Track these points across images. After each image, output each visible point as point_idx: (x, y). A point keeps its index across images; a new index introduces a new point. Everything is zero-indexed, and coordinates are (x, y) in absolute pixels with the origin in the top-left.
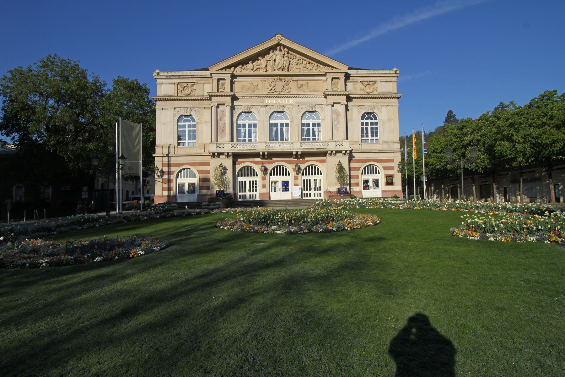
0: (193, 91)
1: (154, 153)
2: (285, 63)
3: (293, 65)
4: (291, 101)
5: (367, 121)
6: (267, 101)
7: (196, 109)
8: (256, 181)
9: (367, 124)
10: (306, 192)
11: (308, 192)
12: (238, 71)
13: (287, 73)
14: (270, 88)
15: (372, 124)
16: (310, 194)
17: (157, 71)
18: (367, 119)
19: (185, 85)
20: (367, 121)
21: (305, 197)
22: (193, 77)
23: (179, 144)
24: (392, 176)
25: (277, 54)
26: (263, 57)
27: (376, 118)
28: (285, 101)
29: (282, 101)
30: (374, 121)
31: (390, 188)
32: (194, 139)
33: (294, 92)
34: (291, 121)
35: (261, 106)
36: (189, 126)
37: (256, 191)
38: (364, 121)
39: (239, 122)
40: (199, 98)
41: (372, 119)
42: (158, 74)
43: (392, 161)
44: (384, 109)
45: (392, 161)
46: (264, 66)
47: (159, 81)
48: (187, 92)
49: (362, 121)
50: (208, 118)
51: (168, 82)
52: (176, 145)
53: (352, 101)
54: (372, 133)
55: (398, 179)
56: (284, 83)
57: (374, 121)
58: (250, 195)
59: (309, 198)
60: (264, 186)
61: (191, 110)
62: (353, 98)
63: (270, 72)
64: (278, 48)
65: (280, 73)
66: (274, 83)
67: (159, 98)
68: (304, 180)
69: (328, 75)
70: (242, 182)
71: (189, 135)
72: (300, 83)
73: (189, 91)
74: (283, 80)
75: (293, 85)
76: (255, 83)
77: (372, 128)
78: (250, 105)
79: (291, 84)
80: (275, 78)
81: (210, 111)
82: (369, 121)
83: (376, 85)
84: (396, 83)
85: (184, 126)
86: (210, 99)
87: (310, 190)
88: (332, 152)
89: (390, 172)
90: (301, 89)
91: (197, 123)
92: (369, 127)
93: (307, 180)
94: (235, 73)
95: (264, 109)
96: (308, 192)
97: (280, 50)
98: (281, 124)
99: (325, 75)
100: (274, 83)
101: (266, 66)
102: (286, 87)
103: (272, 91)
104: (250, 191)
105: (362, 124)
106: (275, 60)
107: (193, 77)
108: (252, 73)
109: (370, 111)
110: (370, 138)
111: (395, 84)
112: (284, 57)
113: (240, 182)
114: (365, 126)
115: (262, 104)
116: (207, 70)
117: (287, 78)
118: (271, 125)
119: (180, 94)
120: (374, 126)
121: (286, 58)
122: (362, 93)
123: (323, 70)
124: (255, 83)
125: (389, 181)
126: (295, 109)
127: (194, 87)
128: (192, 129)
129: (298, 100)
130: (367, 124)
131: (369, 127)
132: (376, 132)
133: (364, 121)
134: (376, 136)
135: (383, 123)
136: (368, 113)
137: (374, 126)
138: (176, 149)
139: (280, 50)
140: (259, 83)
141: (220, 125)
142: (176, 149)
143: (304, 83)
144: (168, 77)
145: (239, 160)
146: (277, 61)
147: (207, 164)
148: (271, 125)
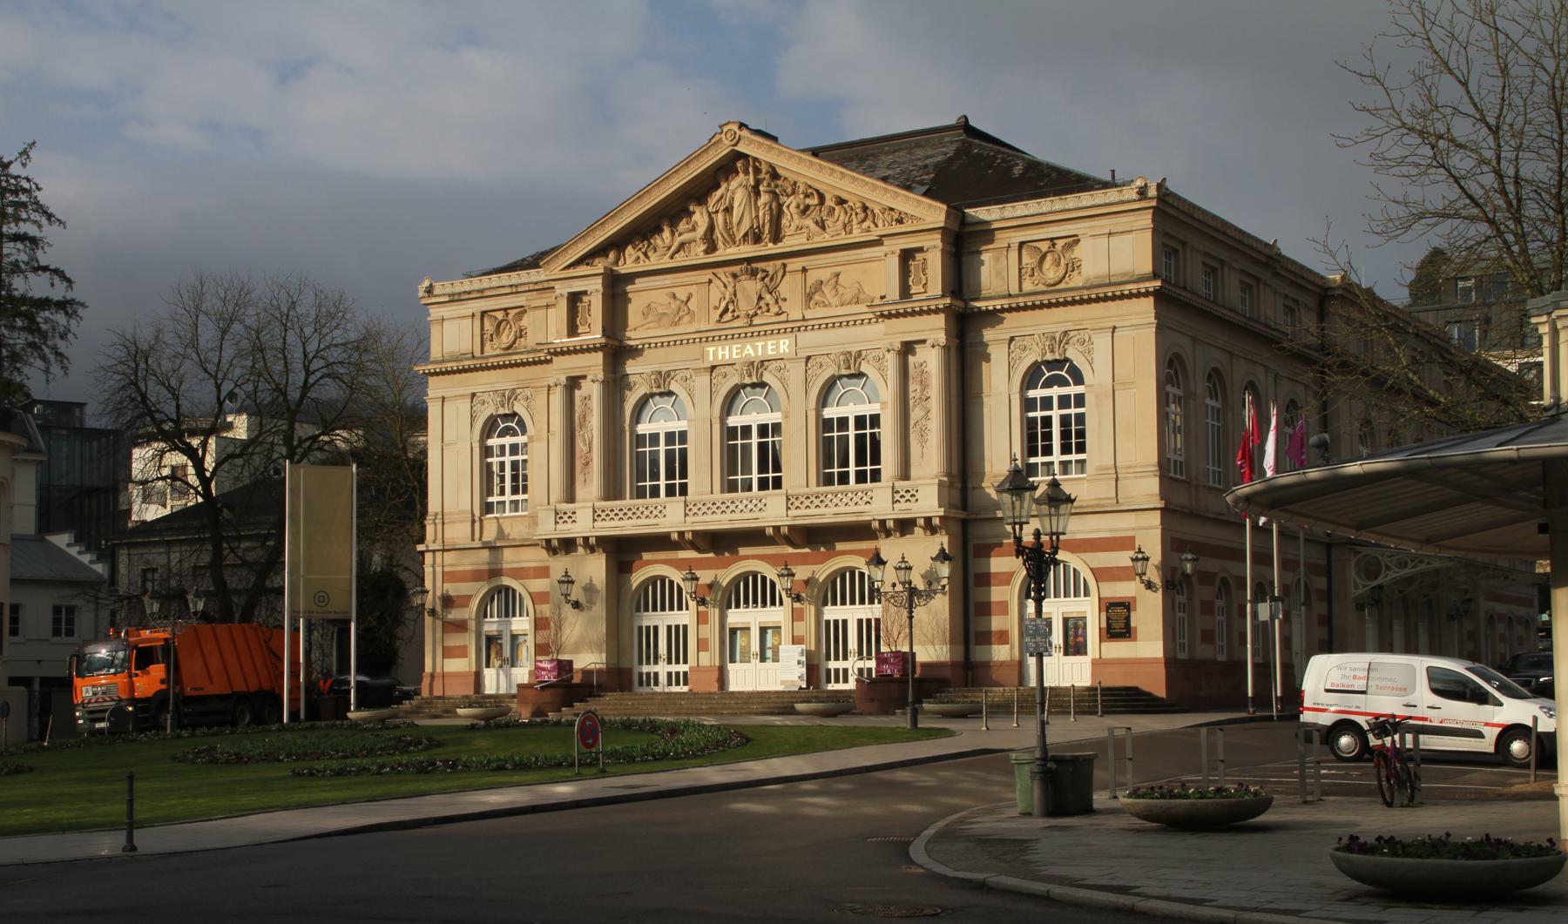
0: (521, 334)
1: (422, 540)
3: (791, 220)
4: (784, 345)
5: (1046, 392)
7: (528, 392)
8: (685, 627)
9: (1047, 403)
11: (841, 664)
12: (630, 261)
13: (770, 248)
15: (1064, 401)
17: (426, 283)
18: (1048, 384)
19: (500, 315)
20: (1046, 392)
21: (837, 681)
22: (515, 290)
24: (1126, 606)
25: (736, 189)
26: (702, 201)
27: (1079, 380)
28: (764, 348)
29: (755, 349)
30: (1072, 390)
32: (525, 491)
34: (786, 416)
37: (685, 662)
38: (1036, 393)
39: (643, 429)
41: (1062, 382)
42: (429, 291)
46: (701, 231)
47: (435, 313)
48: (506, 338)
49: (1032, 394)
52: (477, 513)
53: (1001, 321)
54: (1065, 435)
55: (1149, 612)
56: (759, 285)
57: (1072, 390)
58: (669, 674)
60: (702, 645)
61: (513, 395)
62: (1003, 310)
63: (725, 253)
64: (739, 164)
65: (748, 250)
66: (730, 289)
67: (438, 368)
68: (828, 622)
69: (886, 242)
70: (677, 627)
72: (813, 276)
73: (512, 337)
76: (682, 294)
77: (1065, 421)
78: (664, 370)
80: (736, 269)
82: (1055, 392)
83: (1078, 252)
84: (1148, 235)
87: (845, 658)
88: (882, 522)
90: (817, 297)
92: (1055, 414)
93: (836, 622)
94: (623, 269)
96: (841, 664)
98: (667, 434)
99: (878, 242)
101: (711, 228)
102: (768, 297)
103: (729, 316)
104: (670, 662)
105: (1029, 404)
106: (728, 210)
107: (515, 290)
108: (667, 263)
111: (1146, 240)
112: (758, 194)
115: (700, 365)
116: (533, 263)
117: (770, 266)
119: (488, 351)
120: (1073, 411)
121: (764, 198)
122: (1028, 286)
125: (1119, 625)
126: (796, 372)
127: (524, 323)
129: (808, 339)
131: (1055, 414)
132: (1081, 434)
133: (1036, 393)
134: (1081, 448)
135: (1097, 396)
136: (1052, 365)
137: (1073, 411)
138: (477, 525)
139: (746, 173)
140: (693, 289)
141: (579, 444)
142: (477, 525)
143: (825, 275)
144: (455, 299)
145: (646, 556)
146: (736, 213)
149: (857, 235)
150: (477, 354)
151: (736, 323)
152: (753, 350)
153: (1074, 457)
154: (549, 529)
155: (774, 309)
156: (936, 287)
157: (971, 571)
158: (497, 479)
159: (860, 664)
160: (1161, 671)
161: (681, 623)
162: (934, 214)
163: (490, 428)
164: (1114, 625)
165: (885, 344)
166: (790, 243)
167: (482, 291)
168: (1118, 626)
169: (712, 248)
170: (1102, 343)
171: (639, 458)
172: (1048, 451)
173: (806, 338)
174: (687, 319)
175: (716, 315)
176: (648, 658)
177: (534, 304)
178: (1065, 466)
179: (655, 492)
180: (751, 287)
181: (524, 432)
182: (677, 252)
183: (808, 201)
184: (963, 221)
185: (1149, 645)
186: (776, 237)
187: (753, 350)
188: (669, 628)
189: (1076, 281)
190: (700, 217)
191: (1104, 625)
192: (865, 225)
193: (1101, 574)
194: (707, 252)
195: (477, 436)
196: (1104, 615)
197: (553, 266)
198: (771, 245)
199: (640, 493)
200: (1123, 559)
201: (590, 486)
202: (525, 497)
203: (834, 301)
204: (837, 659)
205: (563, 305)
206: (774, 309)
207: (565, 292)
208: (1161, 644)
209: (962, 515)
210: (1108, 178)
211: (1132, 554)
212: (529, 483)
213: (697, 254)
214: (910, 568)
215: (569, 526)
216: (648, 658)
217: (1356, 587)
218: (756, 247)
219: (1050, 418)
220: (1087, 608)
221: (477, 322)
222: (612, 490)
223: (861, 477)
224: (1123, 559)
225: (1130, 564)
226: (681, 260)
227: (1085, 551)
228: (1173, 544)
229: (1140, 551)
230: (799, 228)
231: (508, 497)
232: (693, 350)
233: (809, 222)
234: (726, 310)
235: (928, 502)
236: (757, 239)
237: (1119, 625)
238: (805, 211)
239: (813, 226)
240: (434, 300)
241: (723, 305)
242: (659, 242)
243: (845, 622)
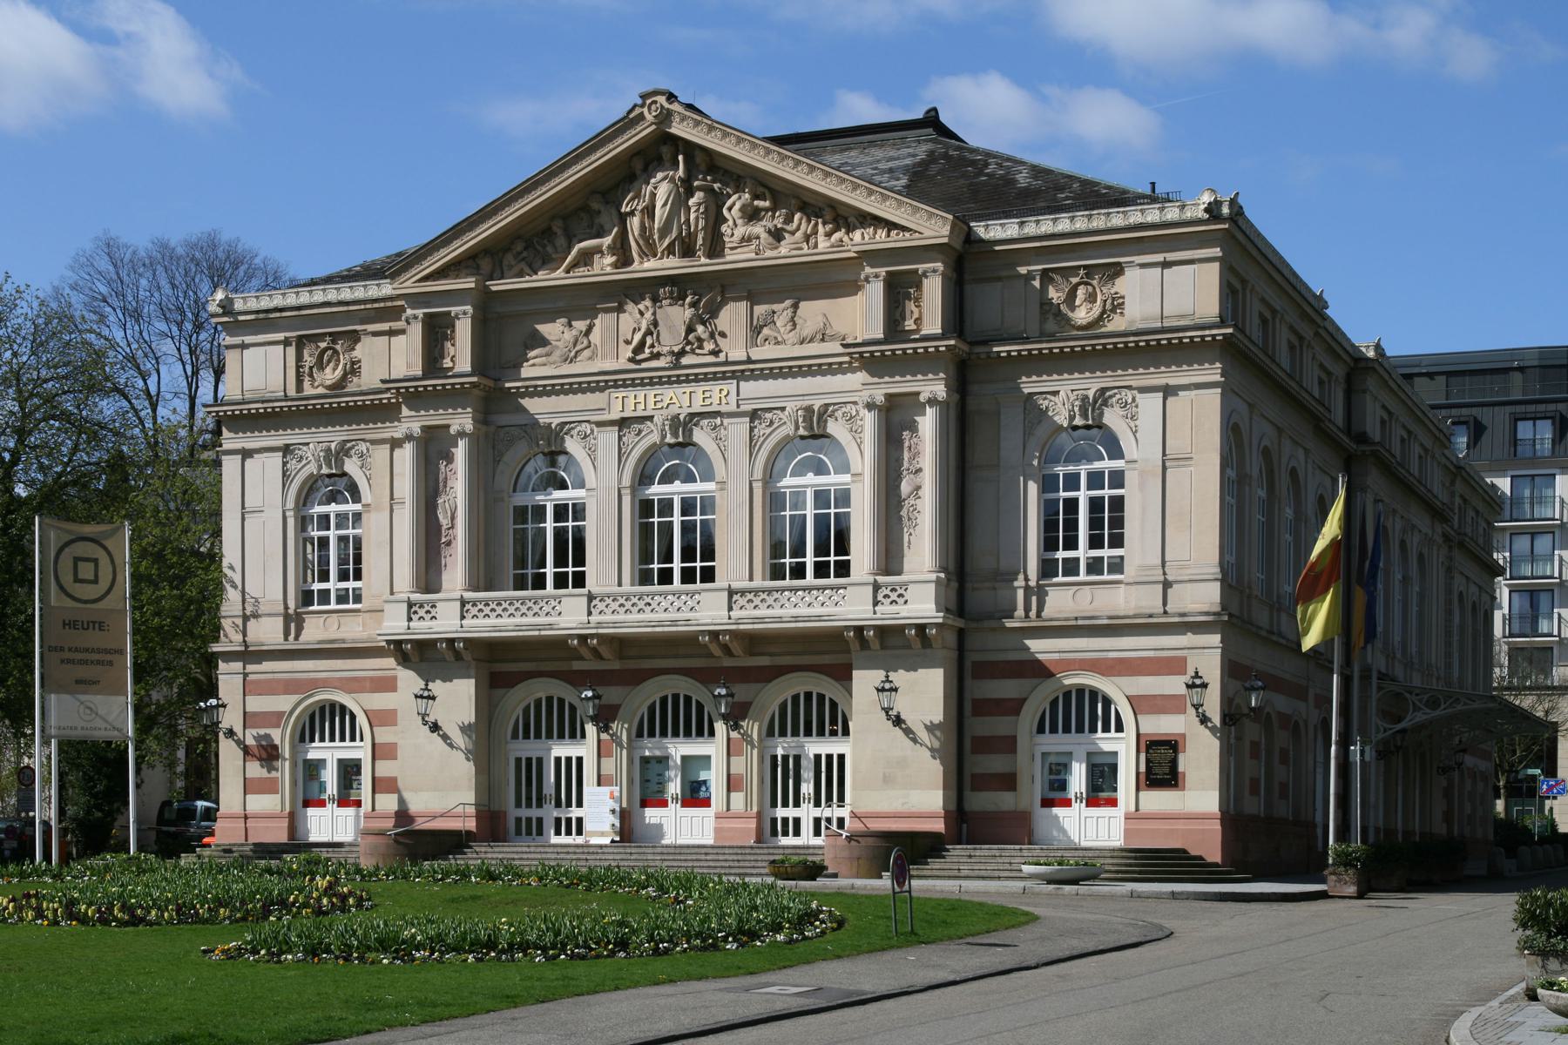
0: (353, 369)
2: (692, 216)
3: (735, 228)
4: (718, 395)
6: (623, 403)
10: (781, 812)
16: (797, 821)
23: (307, 598)
31: (1158, 800)
32: (358, 576)
35: (600, 424)
36: (342, 519)
43: (1173, 665)
48: (331, 375)
54: (1095, 523)
55: (1202, 759)
59: (789, 841)
61: (344, 451)
66: (648, 315)
75: (733, 316)
77: (1096, 505)
85: (324, 521)
92: (1083, 495)
95: (611, 435)
106: (650, 211)
110: (1083, 552)
113: (558, 760)
115: (606, 417)
118: (645, 507)
119: (308, 390)
123: (861, 239)
125: (1161, 766)
126: (738, 430)
127: (358, 352)
130: (1072, 482)
131: (1083, 495)
132: (1118, 522)
134: (1117, 541)
137: (1107, 492)
147: (388, 685)
148: (645, 507)
150: (292, 392)
151: (661, 363)
152: (682, 400)
153: (1106, 553)
154: (395, 624)
155: (709, 346)
156: (933, 324)
157: (968, 697)
158: (325, 564)
159: (817, 812)
160: (1217, 826)
162: (933, 227)
163: (308, 493)
164: (1156, 770)
165: (864, 396)
166: (737, 257)
168: (1162, 771)
169: (624, 260)
171: (520, 537)
172: (1071, 544)
173: (749, 388)
174: (587, 353)
175: (627, 352)
176: (529, 799)
178: (1095, 566)
179: (540, 583)
180: (677, 316)
181: (356, 497)
184: (970, 239)
185: (1200, 796)
186: (715, 247)
187: (682, 400)
188: (518, 760)
189: (1116, 324)
191: (1143, 768)
192: (837, 236)
193: (1140, 704)
194: (615, 265)
195: (290, 504)
196: (1143, 756)
198: (703, 260)
199: (520, 584)
200: (1174, 685)
201: (455, 573)
202: (358, 584)
203: (792, 337)
204: (785, 805)
205: (416, 330)
206: (709, 346)
208: (1216, 794)
209: (960, 623)
210: (1148, 191)
211: (1187, 678)
212: (364, 566)
213: (604, 268)
214: (896, 690)
216: (529, 799)
217: (1378, 732)
218: (685, 262)
219: (1076, 500)
220: (1123, 748)
221: (291, 351)
222: (484, 577)
223: (688, 576)
224: (1174, 685)
225: (1183, 690)
227: (1120, 674)
228: (1233, 669)
229: (1197, 676)
230: (747, 240)
231: (333, 585)
233: (758, 229)
234: (642, 344)
235: (920, 604)
236: (688, 251)
237: (1161, 766)
238: (752, 215)
239: (764, 235)
241: (638, 337)
242: (549, 249)
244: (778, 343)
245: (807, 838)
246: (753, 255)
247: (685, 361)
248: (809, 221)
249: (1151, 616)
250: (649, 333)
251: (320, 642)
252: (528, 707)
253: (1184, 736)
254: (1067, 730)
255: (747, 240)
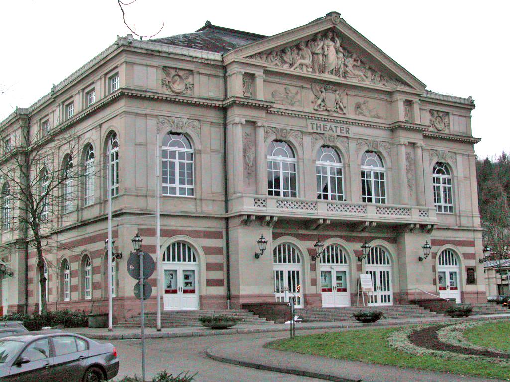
7: (197, 123)
13: (341, 80)
14: (319, 102)
30: (446, 176)
33: (351, 116)
36: (182, 156)
38: (436, 175)
40: (206, 103)
44: (459, 159)
45: (471, 244)
48: (178, 87)
50: (217, 144)
51: (145, 62)
64: (330, 35)
71: (182, 174)
74: (337, 92)
75: (349, 102)
79: (345, 101)
81: (222, 130)
85: (173, 154)
86: (224, 110)
89: (472, 263)
91: (200, 152)
97: (333, 40)
100: (323, 94)
109: (443, 161)
114: (447, 185)
124: (293, 90)
128: (186, 161)
149: (379, 86)
161: (296, 270)
167: (169, 53)
170: (459, 159)
174: (298, 104)
177: (202, 71)
182: (296, 68)
183: (355, 63)
189: (447, 131)
190: (306, 52)
194: (312, 72)
197: (240, 53)
198: (342, 79)
207: (243, 71)
213: (307, 72)
215: (262, 208)
226: (298, 72)
232: (302, 122)
236: (336, 71)
240: (133, 49)
243: (282, 272)
244: (364, 116)
245: (379, 304)
246: (357, 81)
247: (335, 115)
248: (372, 74)
249: (468, 227)
250: (323, 101)
251: (182, 212)
252: (276, 249)
253: (475, 267)
254: (289, 261)
255: (355, 76)
